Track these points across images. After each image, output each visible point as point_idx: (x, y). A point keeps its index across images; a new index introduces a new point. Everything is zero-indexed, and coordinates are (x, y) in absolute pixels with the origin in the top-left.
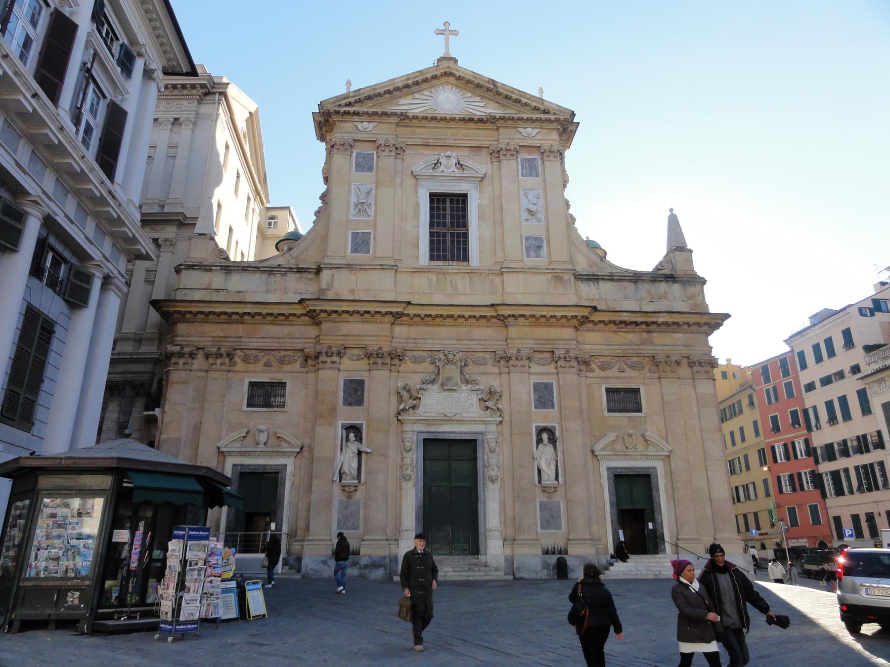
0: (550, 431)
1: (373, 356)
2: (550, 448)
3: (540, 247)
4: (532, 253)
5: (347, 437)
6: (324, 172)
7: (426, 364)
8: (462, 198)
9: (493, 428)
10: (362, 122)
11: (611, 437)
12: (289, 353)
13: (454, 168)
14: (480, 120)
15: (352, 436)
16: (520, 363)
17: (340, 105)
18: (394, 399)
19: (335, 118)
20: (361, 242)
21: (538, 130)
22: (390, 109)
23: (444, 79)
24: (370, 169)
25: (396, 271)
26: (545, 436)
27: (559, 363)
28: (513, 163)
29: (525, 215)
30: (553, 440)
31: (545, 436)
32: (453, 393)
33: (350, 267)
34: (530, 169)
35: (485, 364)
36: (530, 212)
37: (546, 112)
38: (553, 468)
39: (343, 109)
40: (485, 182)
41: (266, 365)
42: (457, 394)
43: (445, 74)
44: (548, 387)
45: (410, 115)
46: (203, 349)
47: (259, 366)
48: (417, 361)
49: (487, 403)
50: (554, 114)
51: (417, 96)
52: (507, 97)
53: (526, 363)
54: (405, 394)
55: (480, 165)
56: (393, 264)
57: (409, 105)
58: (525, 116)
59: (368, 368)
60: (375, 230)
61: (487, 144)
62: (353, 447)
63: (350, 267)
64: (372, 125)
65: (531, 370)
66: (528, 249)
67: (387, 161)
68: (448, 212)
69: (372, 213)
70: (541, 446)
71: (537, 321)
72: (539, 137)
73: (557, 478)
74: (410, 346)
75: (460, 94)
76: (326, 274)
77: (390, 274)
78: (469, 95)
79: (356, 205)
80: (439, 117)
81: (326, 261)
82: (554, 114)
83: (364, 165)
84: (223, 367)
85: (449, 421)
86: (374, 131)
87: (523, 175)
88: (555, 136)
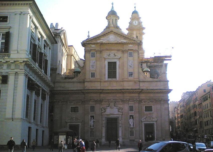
0: (132, 116)
1: (96, 101)
2: (132, 119)
3: (132, 75)
4: (130, 76)
5: (91, 118)
6: (84, 57)
7: (107, 103)
8: (115, 63)
9: (121, 116)
10: (92, 45)
11: (145, 117)
12: (78, 101)
13: (113, 56)
14: (119, 43)
15: (92, 118)
16: (127, 102)
17: (87, 42)
18: (100, 110)
19: (86, 44)
20: (93, 75)
21: (133, 45)
22: (98, 41)
23: (111, 32)
24: (95, 57)
25: (101, 82)
26: (131, 117)
27: (135, 102)
28: (126, 54)
29: (129, 67)
30: (133, 118)
31: (131, 117)
32: (113, 109)
33: (91, 81)
34: (131, 55)
35: (119, 102)
36: (130, 66)
37: (134, 41)
38: (133, 124)
39: (88, 42)
40: (120, 59)
41: (74, 103)
42: (114, 109)
43: (111, 31)
44: (132, 107)
45: (103, 43)
46: (61, 100)
47: (73, 104)
48: (106, 102)
49: (119, 111)
50: (137, 41)
51: (105, 37)
52: (126, 37)
53: (128, 102)
54: (103, 109)
55: (119, 55)
56: (100, 80)
57: (103, 40)
58: (130, 42)
59: (95, 103)
60: (96, 72)
61: (121, 49)
62: (93, 120)
63: (91, 81)
64: (95, 45)
65: (129, 103)
66: (129, 75)
67: (98, 55)
68: (112, 66)
69: (95, 68)
70: (130, 119)
71: (130, 93)
72: (133, 47)
73: (133, 126)
74: (104, 99)
75: (115, 36)
76: (86, 84)
77: (99, 83)
78: (117, 36)
79: (92, 66)
80: (110, 43)
81: (86, 80)
82: (137, 41)
83: (93, 56)
84: (65, 104)
85: (112, 115)
86: (95, 47)
87: (129, 57)
88: (137, 46)
